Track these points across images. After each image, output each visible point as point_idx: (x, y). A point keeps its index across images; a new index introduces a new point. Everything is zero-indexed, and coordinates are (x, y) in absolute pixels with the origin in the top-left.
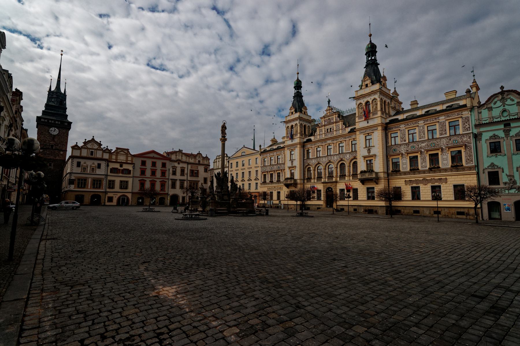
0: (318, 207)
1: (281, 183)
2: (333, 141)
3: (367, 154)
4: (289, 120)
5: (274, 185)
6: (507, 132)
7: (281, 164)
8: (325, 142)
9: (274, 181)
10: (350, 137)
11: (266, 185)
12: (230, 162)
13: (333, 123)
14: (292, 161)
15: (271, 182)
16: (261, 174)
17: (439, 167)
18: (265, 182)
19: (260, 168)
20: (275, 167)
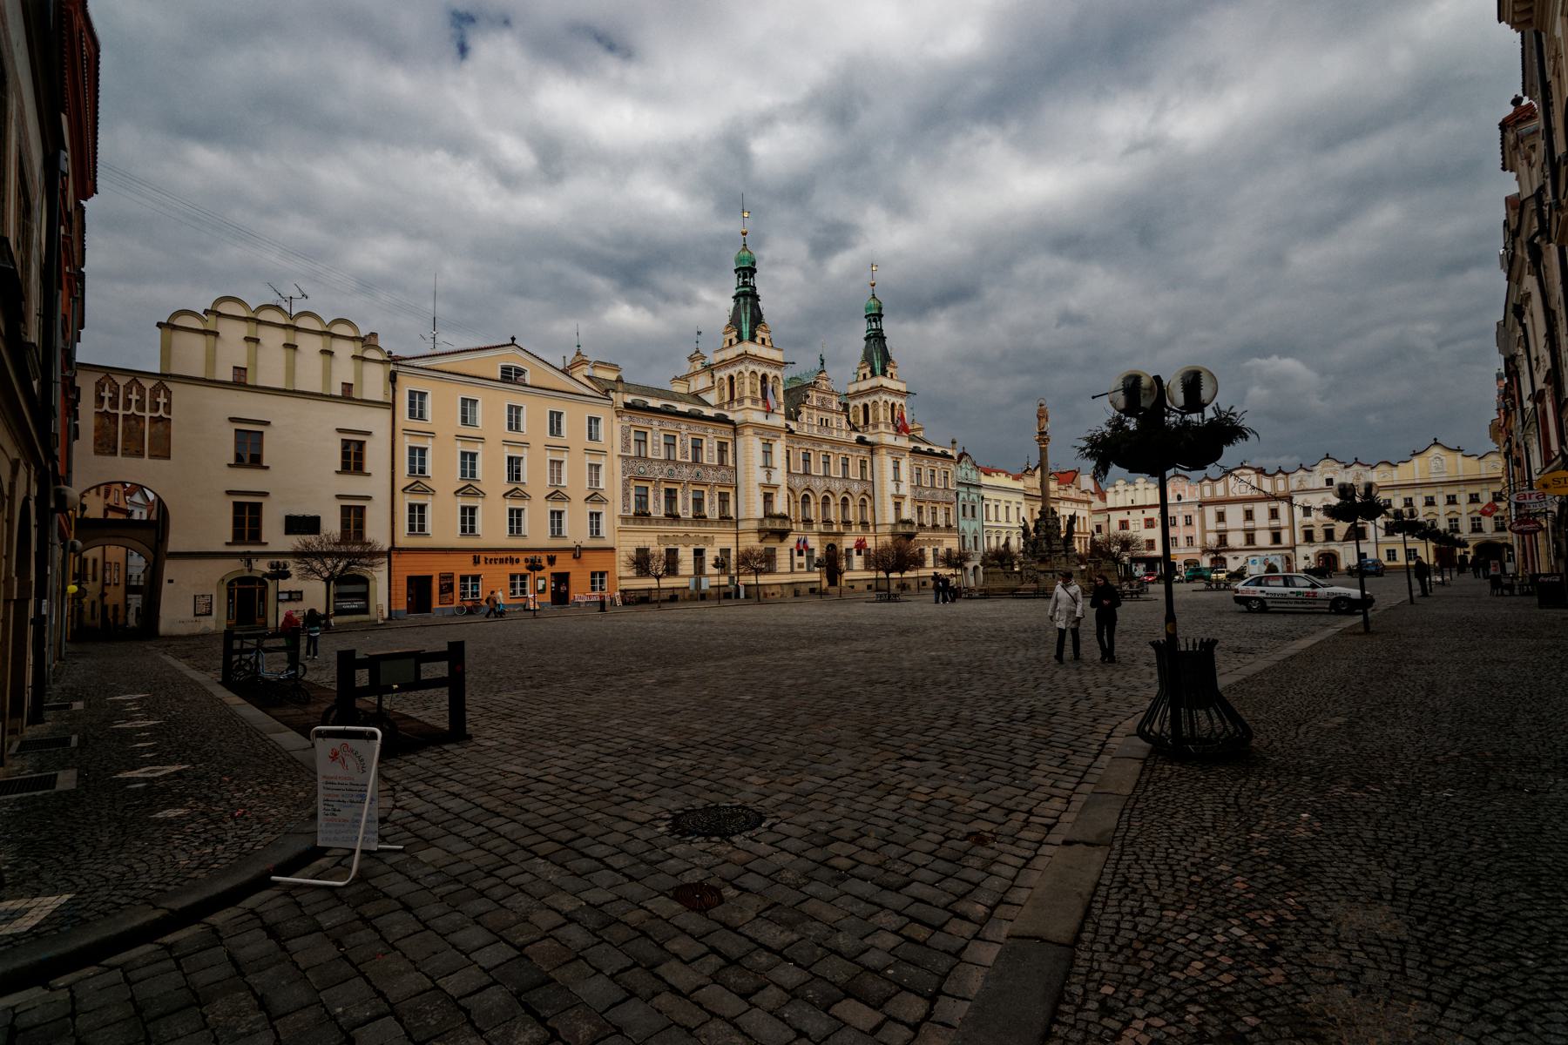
0: (811, 586)
1: (679, 521)
2: (833, 448)
3: (895, 493)
4: (755, 356)
5: (683, 528)
6: (969, 495)
7: (707, 466)
8: (820, 446)
9: (684, 513)
10: (858, 451)
11: (650, 524)
12: (406, 384)
13: (832, 411)
14: (768, 467)
15: (673, 517)
16: (626, 484)
17: (705, 517)
18: (642, 515)
19: (618, 464)
20: (686, 471)
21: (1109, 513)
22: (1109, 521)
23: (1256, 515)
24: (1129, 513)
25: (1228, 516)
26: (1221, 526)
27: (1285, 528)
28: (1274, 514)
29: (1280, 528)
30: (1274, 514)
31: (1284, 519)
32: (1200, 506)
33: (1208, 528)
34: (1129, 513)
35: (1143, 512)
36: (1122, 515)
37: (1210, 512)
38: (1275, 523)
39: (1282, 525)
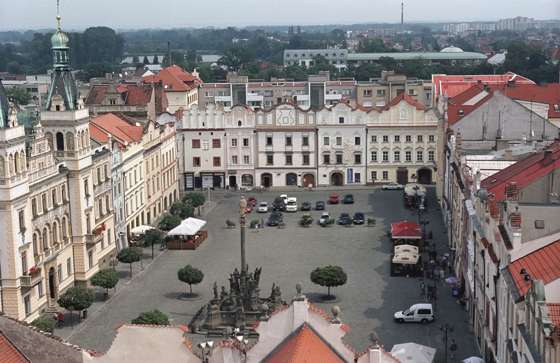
21: (184, 133)
22: (184, 139)
23: (294, 141)
24: (200, 134)
25: (274, 141)
26: (270, 149)
27: (313, 152)
28: (305, 141)
29: (309, 153)
30: (305, 141)
31: (311, 147)
32: (255, 132)
33: (260, 150)
34: (200, 134)
35: (212, 134)
36: (195, 136)
37: (262, 138)
38: (305, 148)
39: (310, 150)
